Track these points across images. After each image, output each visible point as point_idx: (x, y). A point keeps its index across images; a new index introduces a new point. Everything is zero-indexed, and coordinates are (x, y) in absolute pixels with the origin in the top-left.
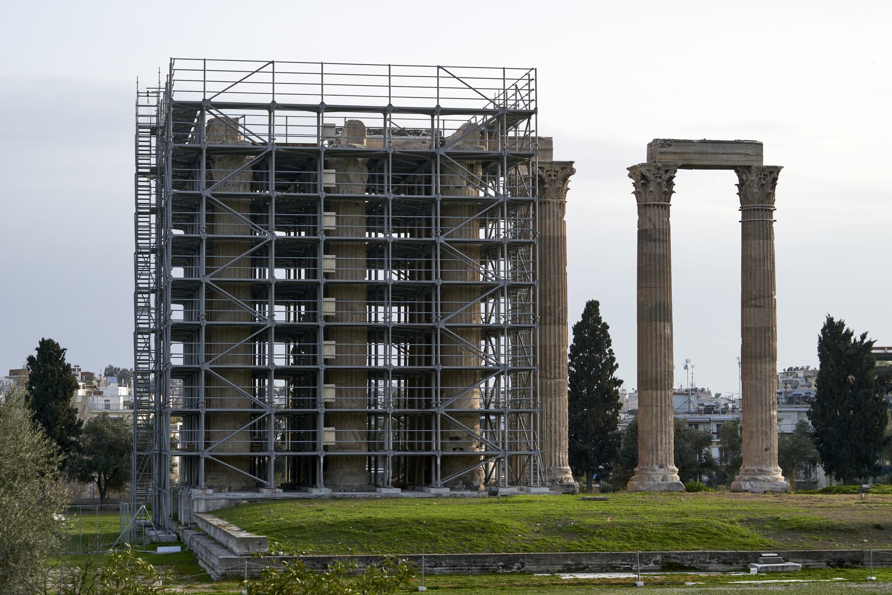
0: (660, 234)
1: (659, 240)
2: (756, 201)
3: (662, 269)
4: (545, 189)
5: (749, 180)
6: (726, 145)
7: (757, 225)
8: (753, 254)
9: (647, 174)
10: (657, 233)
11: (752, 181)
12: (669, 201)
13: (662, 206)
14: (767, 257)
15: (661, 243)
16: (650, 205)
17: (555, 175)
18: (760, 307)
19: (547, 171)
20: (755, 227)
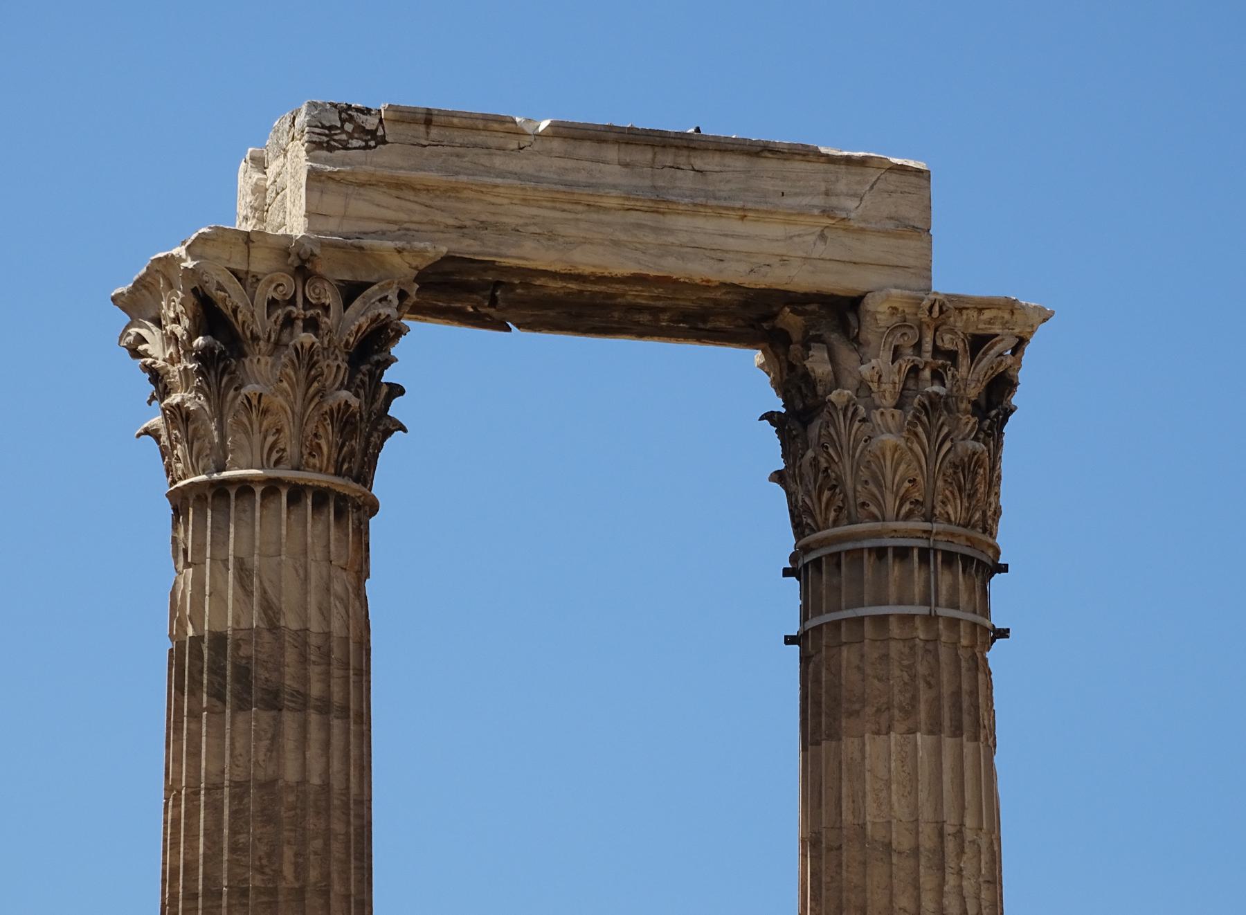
1: (302, 701)
2: (891, 503)
3: (313, 874)
7: (895, 648)
8: (871, 813)
9: (232, 296)
10: (290, 656)
11: (863, 387)
12: (365, 476)
13: (321, 497)
16: (244, 487)
20: (885, 657)
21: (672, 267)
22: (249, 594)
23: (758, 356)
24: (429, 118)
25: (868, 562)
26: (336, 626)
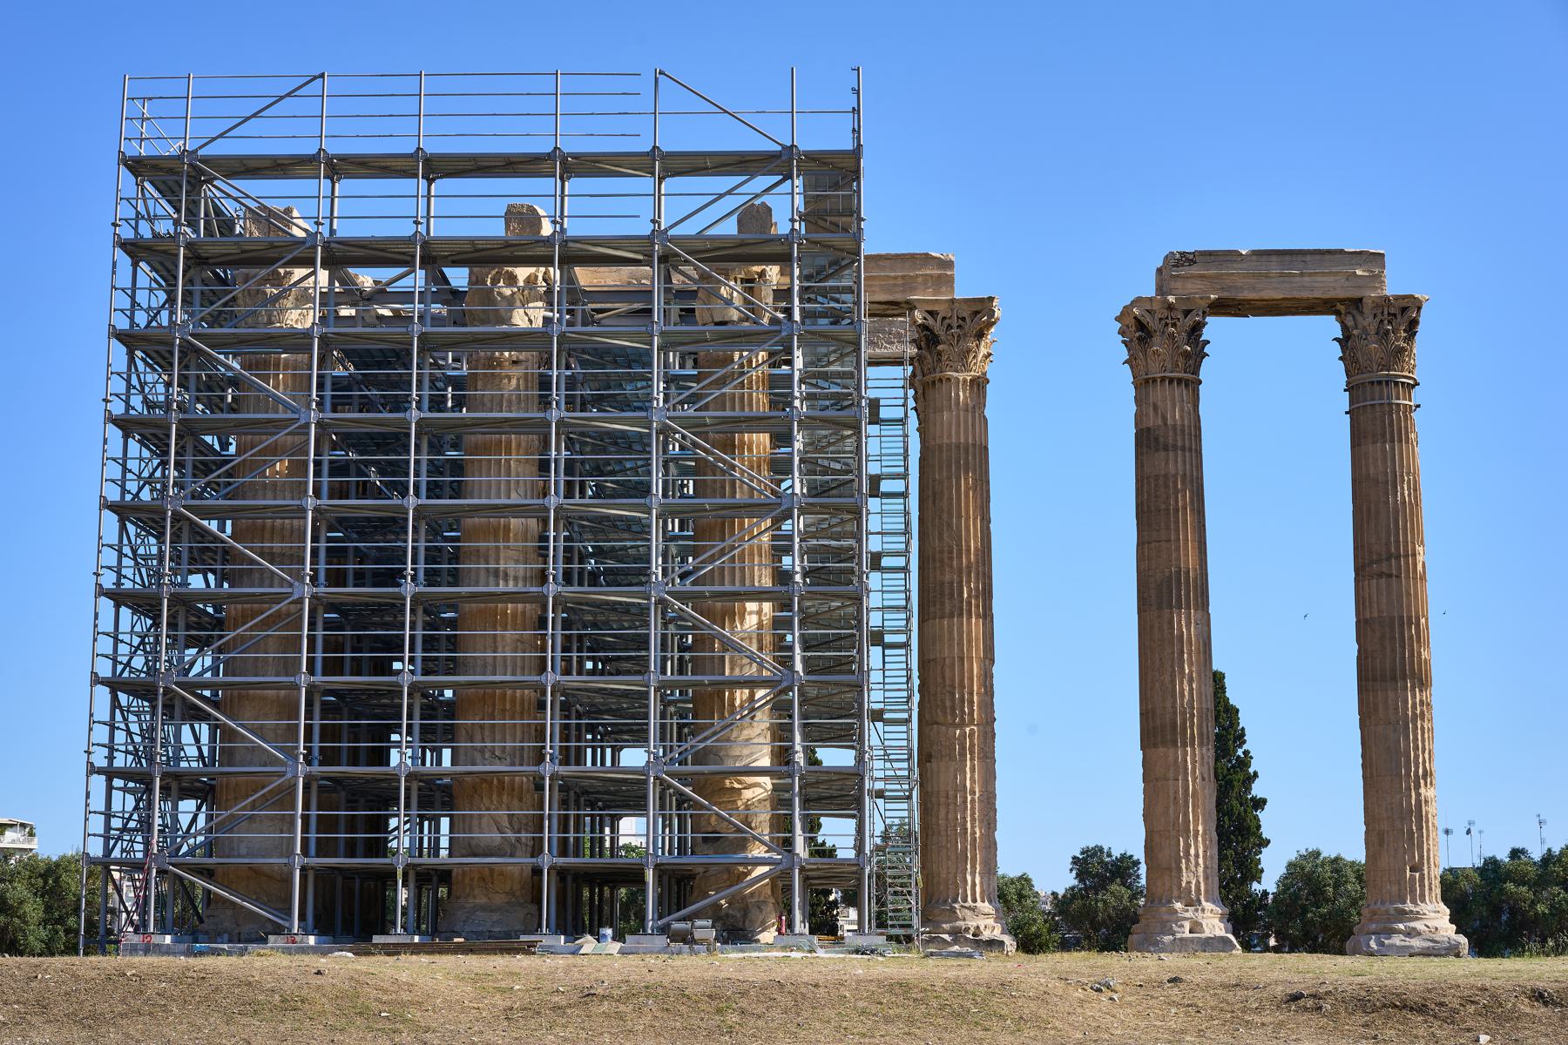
0: (1175, 434)
1: (1175, 448)
2: (1375, 367)
4: (939, 354)
5: (1360, 326)
6: (1308, 258)
9: (1147, 319)
10: (1171, 433)
12: (1196, 371)
13: (1180, 381)
14: (1402, 476)
15: (1180, 452)
16: (1154, 380)
17: (959, 327)
18: (1390, 576)
19: (944, 318)
21: (1296, 294)
22: (1157, 414)
23: (1334, 317)
24: (1210, 253)
25: (1368, 387)
26: (1186, 423)
